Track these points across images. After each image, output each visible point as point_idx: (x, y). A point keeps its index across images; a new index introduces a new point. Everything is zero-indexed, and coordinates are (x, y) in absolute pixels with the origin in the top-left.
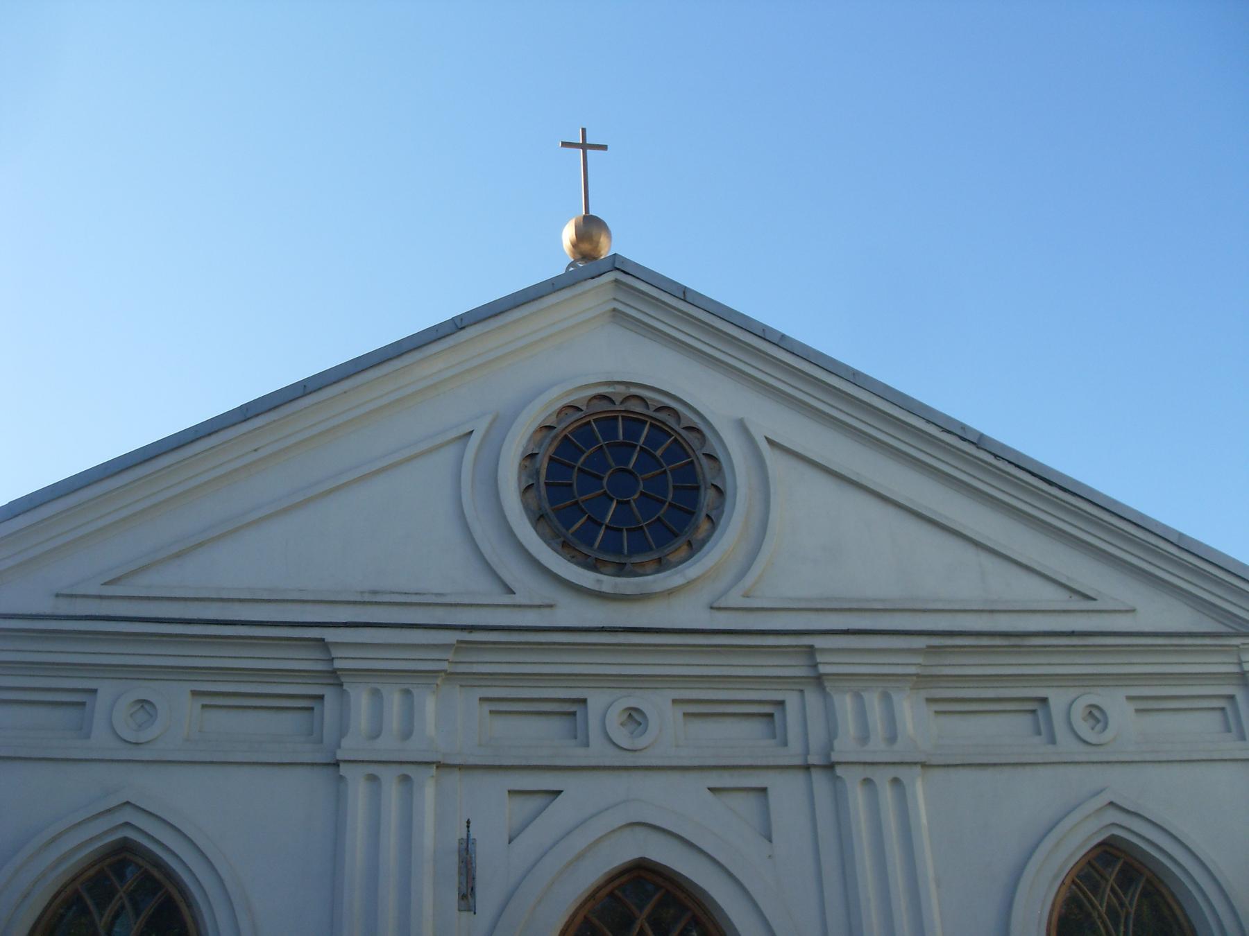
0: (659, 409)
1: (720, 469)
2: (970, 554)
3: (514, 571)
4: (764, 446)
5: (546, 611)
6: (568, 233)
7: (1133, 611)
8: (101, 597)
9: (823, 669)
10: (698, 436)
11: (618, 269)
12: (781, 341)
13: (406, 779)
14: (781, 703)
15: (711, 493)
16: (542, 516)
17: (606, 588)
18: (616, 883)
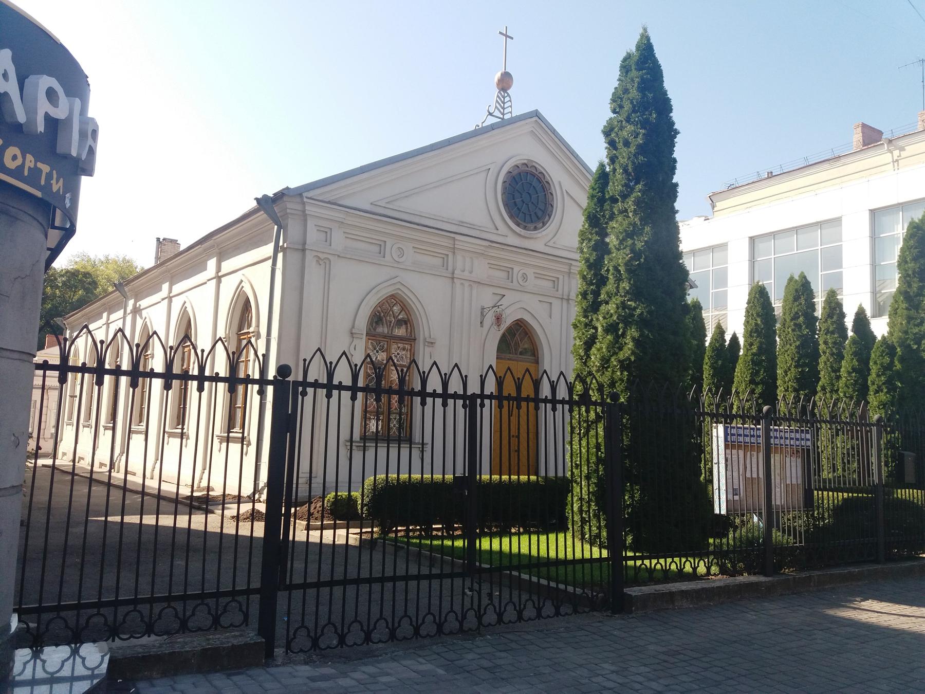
0: (539, 173)
4: (565, 193)
6: (498, 75)
8: (385, 207)
9: (572, 271)
12: (577, 157)
13: (470, 285)
14: (558, 278)
17: (522, 234)
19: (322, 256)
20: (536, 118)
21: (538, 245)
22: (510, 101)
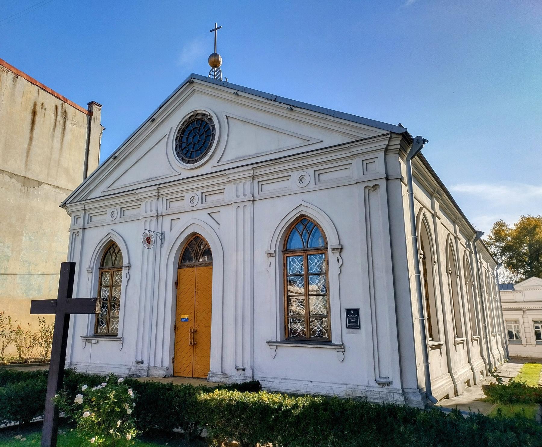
7: (322, 141)
21: (207, 169)
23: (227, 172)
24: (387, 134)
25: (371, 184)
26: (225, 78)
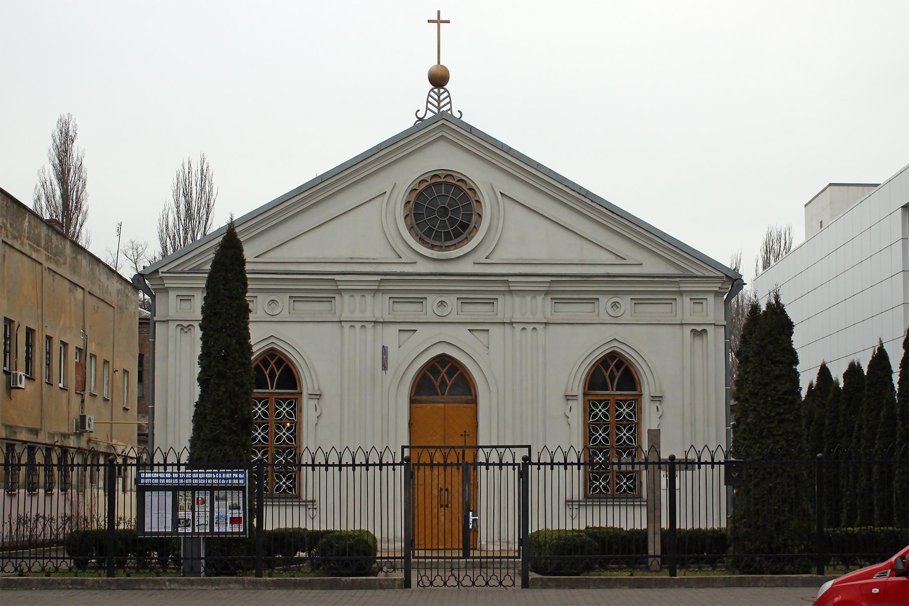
1: (481, 206)
2: (578, 240)
3: (401, 249)
5: (414, 264)
7: (641, 264)
10: (473, 191)
11: (444, 119)
12: (509, 150)
15: (477, 216)
16: (412, 227)
17: (435, 257)
18: (436, 360)
19: (185, 324)
20: (443, 121)
21: (466, 267)
22: (449, 96)
23: (510, 279)
24: (722, 278)
25: (699, 329)
26: (459, 111)
